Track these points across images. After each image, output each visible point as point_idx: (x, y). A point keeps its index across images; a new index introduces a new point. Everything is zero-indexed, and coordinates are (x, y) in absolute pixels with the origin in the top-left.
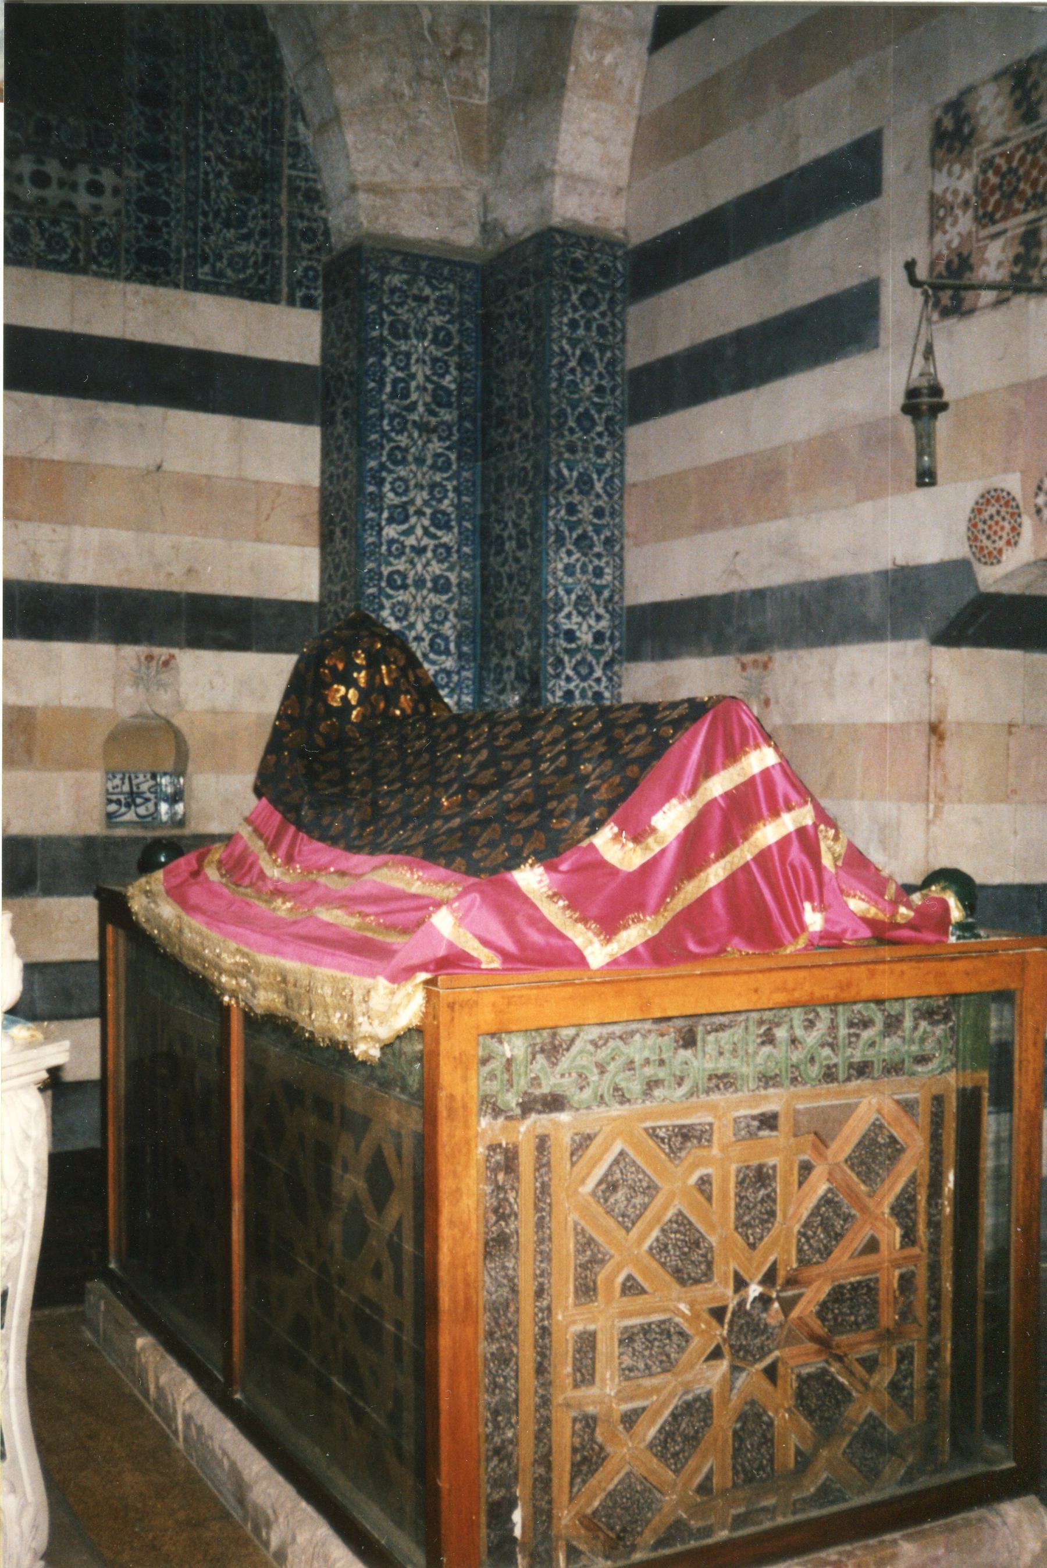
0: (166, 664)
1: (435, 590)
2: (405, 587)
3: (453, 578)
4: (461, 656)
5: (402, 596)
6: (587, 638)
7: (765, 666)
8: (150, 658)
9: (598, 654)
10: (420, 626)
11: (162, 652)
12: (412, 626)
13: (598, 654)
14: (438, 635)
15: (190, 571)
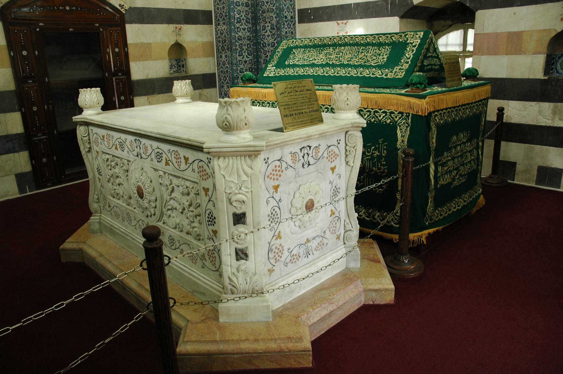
0: (180, 29)
1: (246, 6)
2: (239, 6)
3: (249, 2)
4: (253, 24)
5: (239, 8)
6: (290, 18)
7: (346, 24)
8: (176, 28)
9: (292, 21)
10: (243, 16)
11: (179, 26)
12: (242, 16)
13: (292, 22)
14: (247, 18)
15: (183, 3)
